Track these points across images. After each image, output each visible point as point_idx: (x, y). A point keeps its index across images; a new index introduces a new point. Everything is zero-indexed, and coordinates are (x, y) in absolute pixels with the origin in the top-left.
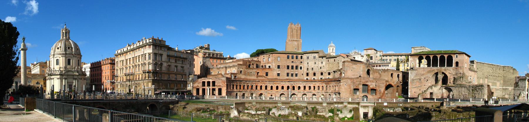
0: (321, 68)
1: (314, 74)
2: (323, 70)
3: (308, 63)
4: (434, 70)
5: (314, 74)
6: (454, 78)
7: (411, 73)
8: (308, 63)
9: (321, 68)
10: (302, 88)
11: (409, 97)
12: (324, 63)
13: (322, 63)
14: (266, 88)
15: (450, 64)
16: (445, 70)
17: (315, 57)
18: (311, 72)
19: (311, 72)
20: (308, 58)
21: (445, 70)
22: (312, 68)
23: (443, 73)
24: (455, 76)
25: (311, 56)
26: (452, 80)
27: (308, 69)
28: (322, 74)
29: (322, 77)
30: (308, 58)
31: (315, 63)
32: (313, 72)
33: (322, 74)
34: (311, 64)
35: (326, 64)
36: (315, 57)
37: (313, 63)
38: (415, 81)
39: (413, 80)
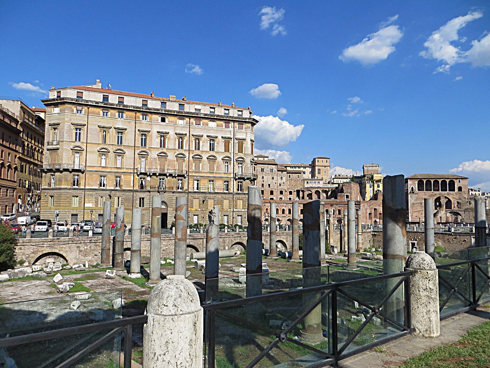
0: (280, 185)
1: (272, 193)
2: (283, 187)
3: (263, 177)
4: (436, 194)
5: (272, 193)
6: (458, 203)
7: (411, 197)
8: (263, 177)
9: (280, 185)
10: (287, 212)
11: (410, 221)
12: (284, 179)
13: (282, 178)
14: (283, 213)
15: (452, 189)
16: (448, 194)
17: (272, 170)
18: (267, 190)
19: (267, 190)
20: (262, 170)
21: (448, 194)
22: (269, 185)
23: (446, 197)
24: (459, 201)
25: (267, 168)
26: (456, 205)
27: (263, 185)
28: (281, 193)
29: (281, 196)
30: (262, 170)
31: (273, 178)
32: (270, 189)
33: (281, 193)
34: (268, 179)
35: (287, 181)
36: (272, 170)
37: (271, 177)
38: (416, 205)
39: (414, 204)
